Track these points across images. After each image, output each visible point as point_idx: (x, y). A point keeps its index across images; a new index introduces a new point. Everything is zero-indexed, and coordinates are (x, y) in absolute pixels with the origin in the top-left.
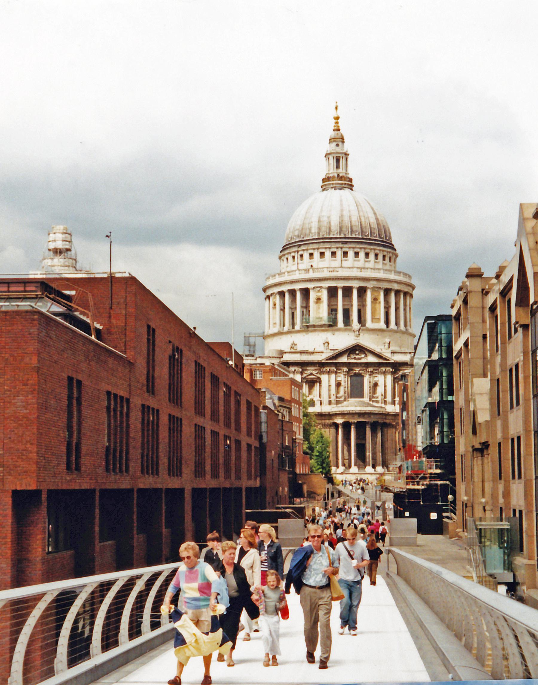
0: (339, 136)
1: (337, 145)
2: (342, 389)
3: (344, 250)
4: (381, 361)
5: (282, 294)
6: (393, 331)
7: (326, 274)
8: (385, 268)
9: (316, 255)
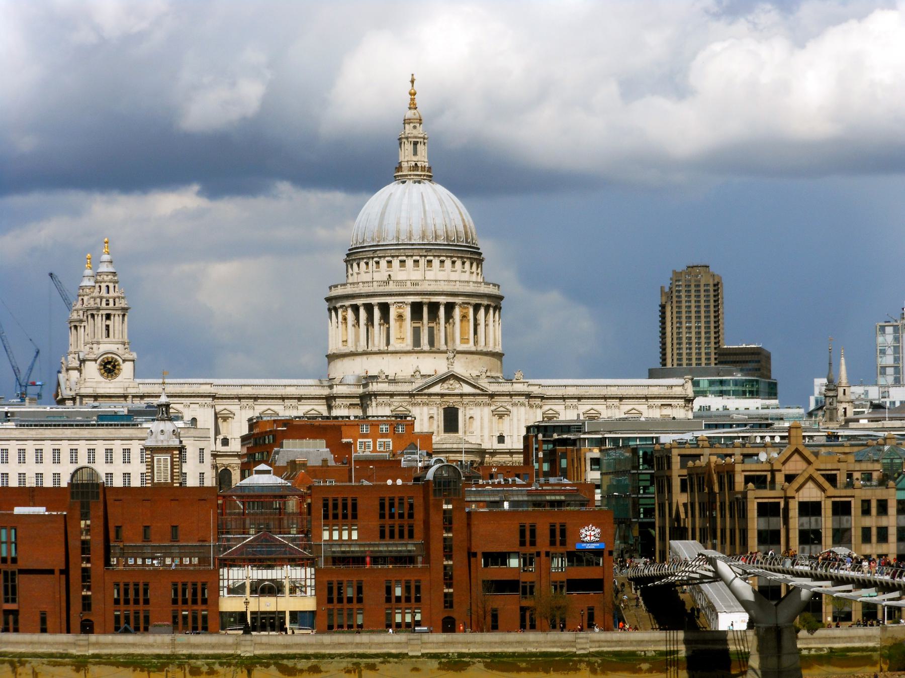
0: (417, 116)
1: (415, 127)
2: (435, 423)
3: (428, 258)
4: (478, 391)
7: (409, 288)
8: (474, 278)
9: (396, 262)
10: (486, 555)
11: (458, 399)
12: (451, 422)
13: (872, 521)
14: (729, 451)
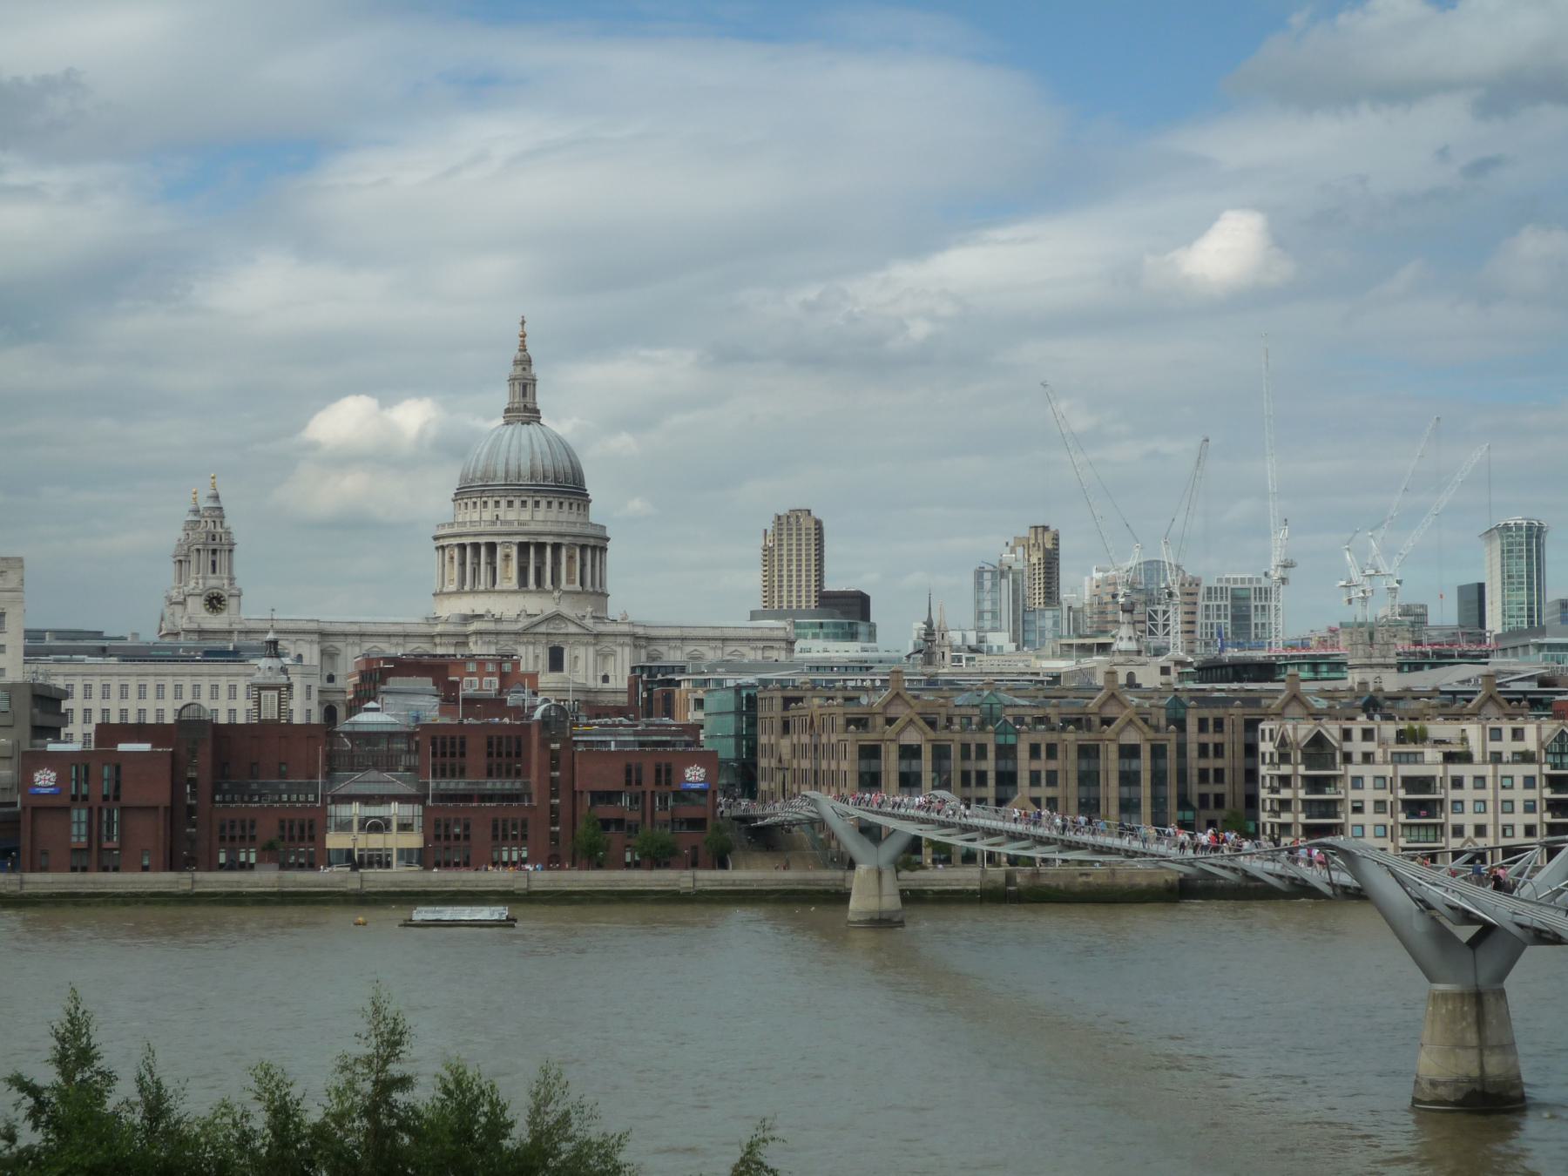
5: (462, 547)
6: (587, 593)
7: (516, 528)
9: (503, 503)
10: (593, 793)
11: (561, 638)
12: (556, 661)
13: (973, 765)
14: (831, 694)
